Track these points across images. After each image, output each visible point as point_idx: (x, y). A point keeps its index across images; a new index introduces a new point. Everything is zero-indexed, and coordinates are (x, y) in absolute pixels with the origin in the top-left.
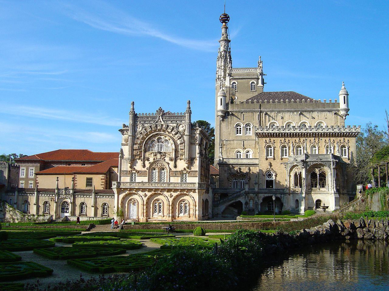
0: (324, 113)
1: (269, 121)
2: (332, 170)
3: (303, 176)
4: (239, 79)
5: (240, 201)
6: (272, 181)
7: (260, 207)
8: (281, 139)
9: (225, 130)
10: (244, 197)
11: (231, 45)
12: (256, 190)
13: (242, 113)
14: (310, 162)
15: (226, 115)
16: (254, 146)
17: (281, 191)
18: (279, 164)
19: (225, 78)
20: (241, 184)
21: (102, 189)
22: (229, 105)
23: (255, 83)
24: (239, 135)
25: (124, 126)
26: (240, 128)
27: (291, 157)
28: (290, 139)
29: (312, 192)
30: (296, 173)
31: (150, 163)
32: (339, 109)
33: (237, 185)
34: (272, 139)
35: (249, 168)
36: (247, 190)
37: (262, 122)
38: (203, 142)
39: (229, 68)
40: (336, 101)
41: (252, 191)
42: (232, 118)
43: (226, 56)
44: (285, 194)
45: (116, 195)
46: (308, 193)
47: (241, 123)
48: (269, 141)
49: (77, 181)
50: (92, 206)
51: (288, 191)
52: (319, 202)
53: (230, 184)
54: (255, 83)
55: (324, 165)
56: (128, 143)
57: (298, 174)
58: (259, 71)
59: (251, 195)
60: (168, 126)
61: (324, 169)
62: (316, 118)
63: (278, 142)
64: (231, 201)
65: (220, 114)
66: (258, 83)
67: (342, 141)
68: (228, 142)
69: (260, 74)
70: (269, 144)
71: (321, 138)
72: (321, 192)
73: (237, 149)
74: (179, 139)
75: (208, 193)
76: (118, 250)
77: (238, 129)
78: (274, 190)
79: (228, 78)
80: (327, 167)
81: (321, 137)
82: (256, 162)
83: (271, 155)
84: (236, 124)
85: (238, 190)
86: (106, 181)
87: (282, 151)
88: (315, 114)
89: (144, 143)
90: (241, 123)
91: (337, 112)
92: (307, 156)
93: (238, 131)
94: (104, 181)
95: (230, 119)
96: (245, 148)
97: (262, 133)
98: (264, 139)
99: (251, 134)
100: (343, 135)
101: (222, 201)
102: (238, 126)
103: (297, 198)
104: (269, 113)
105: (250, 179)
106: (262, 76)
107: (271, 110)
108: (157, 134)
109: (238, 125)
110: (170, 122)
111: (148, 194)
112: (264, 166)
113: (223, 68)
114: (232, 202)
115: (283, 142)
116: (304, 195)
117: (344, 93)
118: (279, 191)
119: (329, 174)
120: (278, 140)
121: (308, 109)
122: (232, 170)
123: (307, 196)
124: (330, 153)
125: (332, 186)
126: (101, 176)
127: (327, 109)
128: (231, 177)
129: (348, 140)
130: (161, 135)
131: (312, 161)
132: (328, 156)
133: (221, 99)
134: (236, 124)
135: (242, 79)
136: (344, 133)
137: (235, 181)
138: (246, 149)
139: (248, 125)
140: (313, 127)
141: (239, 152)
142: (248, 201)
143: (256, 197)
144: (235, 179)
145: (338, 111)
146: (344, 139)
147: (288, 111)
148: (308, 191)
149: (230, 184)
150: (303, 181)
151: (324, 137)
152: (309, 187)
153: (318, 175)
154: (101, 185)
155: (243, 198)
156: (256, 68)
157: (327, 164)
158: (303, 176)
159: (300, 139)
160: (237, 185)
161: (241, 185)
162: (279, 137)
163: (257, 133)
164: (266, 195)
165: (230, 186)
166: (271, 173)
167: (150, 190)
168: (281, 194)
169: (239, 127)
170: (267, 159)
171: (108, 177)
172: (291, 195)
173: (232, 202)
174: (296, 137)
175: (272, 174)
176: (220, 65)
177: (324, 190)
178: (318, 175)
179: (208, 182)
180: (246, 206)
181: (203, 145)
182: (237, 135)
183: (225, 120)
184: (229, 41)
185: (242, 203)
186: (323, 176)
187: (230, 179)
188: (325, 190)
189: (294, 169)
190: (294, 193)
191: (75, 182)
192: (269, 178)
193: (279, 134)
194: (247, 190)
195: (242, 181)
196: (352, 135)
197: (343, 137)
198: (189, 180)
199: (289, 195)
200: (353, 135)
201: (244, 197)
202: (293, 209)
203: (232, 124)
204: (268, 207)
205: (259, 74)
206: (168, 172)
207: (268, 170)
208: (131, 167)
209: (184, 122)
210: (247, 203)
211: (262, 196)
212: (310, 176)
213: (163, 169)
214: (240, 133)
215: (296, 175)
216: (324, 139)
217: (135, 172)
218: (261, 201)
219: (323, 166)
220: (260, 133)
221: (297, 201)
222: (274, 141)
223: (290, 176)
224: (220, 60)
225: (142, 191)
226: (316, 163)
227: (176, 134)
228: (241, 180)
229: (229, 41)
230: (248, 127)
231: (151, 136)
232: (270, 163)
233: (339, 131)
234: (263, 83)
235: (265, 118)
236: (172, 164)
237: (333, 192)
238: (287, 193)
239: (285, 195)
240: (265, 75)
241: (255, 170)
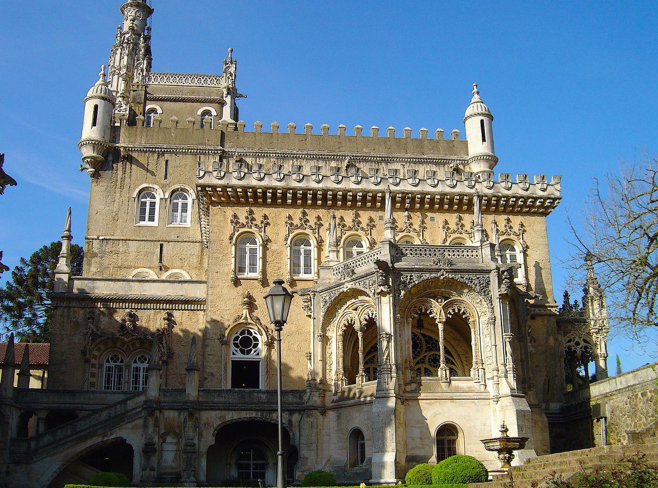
2: (497, 303)
3: (386, 322)
5: (122, 442)
6: (256, 364)
7: (204, 463)
8: (291, 211)
9: (101, 207)
10: (140, 422)
11: (152, 21)
14: (411, 270)
15: (108, 158)
16: (195, 260)
20: (136, 377)
22: (122, 130)
24: (146, 223)
26: (153, 205)
27: (327, 267)
28: (321, 212)
29: (423, 395)
32: (465, 158)
34: (259, 212)
35: (170, 315)
36: (153, 392)
39: (142, 71)
40: (457, 135)
41: (174, 397)
42: (128, 171)
43: (136, 44)
44: (305, 410)
46: (409, 395)
47: (156, 187)
48: (247, 218)
51: (316, 400)
52: (448, 432)
53: (93, 375)
54: (214, 113)
55: (464, 285)
57: (357, 326)
58: (224, 83)
59: (171, 414)
61: (461, 302)
63: (280, 219)
65: (88, 152)
66: (220, 115)
68: (109, 247)
69: (228, 89)
70: (246, 229)
71: (430, 215)
72: (455, 395)
78: (264, 396)
80: (473, 294)
81: (431, 209)
82: (197, 292)
83: (253, 270)
84: (138, 190)
87: (295, 254)
90: (156, 187)
91: (461, 167)
92: (396, 251)
93: (143, 211)
95: (120, 173)
97: (224, 188)
98: (230, 211)
99: (188, 224)
100: (506, 205)
101: (47, 438)
103: (358, 420)
104: (249, 160)
106: (233, 98)
107: (256, 150)
112: (226, 308)
113: (124, 71)
114: (90, 442)
115: (296, 222)
116: (392, 403)
117: (480, 111)
119: (484, 319)
120: (279, 216)
121: (372, 154)
122: (104, 320)
123: (401, 408)
124: (482, 241)
125: (502, 368)
128: (99, 350)
129: (522, 225)
131: (418, 270)
132: (474, 253)
133: (96, 107)
134: (141, 187)
136: (508, 198)
137: (112, 364)
138: (167, 269)
142: (156, 439)
143: (189, 423)
145: (466, 163)
146: (509, 220)
148: (405, 392)
149: (93, 375)
150: (385, 344)
151: (441, 210)
152: (409, 374)
153: (441, 327)
156: (218, 78)
157: (477, 282)
158: (386, 322)
159: (357, 215)
162: (284, 204)
163: (204, 187)
165: (92, 385)
166: (250, 333)
169: (148, 200)
170: (237, 282)
172: (331, 415)
173: (90, 442)
174: (344, 206)
175: (256, 339)
176: (117, 63)
178: (441, 327)
182: (142, 223)
183: (106, 174)
184: (149, 12)
185: (130, 447)
186: (459, 328)
187: (95, 357)
189: (341, 312)
190: (344, 403)
192: (243, 352)
193: (285, 191)
194: (153, 392)
196: (533, 206)
197: (504, 212)
199: (323, 413)
200: (539, 207)
201: (140, 422)
203: (126, 188)
204: (239, 467)
205: (225, 92)
207: (241, 321)
210: (149, 449)
214: (152, 219)
215: (349, 333)
216: (440, 218)
218: (209, 439)
219: (460, 287)
220: (214, 187)
221: (357, 434)
222: (265, 217)
223: (325, 340)
224: (119, 52)
226: (433, 275)
228: (135, 362)
230: (180, 202)
232: (250, 297)
233: (491, 191)
234: (235, 115)
237: (508, 392)
238: (315, 408)
239: (308, 416)
240: (241, 96)
241: (191, 323)
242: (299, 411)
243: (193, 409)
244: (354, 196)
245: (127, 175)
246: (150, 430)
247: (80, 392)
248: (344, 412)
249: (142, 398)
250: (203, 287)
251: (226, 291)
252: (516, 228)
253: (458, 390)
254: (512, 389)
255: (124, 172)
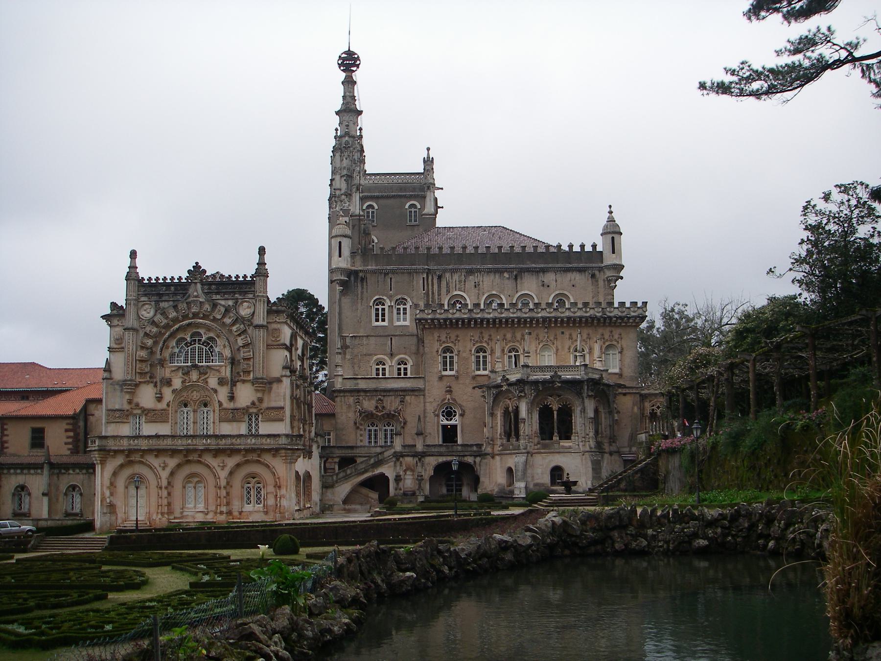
0: (569, 276)
1: (448, 292)
3: (523, 413)
4: (382, 197)
7: (428, 486)
10: (392, 464)
12: (420, 448)
13: (386, 274)
16: (414, 348)
17: (475, 448)
18: (470, 389)
19: (349, 195)
20: (386, 435)
21: (69, 452)
23: (419, 207)
24: (380, 323)
25: (114, 305)
26: (383, 310)
28: (492, 332)
30: (507, 408)
31: (174, 391)
33: (376, 438)
37: (433, 293)
38: (296, 340)
44: (483, 455)
45: (98, 469)
49: (7, 435)
50: (44, 494)
54: (419, 207)
56: (123, 345)
57: (510, 409)
59: (409, 460)
60: (215, 306)
62: (551, 286)
64: (363, 473)
66: (423, 207)
67: (607, 337)
68: (357, 341)
73: (375, 358)
74: (239, 335)
75: (310, 458)
76: (87, 594)
77: (377, 310)
78: (459, 448)
79: (356, 197)
85: (379, 450)
86: (77, 435)
88: (550, 278)
89: (161, 345)
93: (377, 315)
94: (71, 434)
95: (360, 288)
96: (392, 355)
97: (432, 320)
99: (407, 323)
102: (377, 305)
105: (405, 423)
107: (451, 267)
108: (189, 325)
109: (379, 302)
110: (218, 297)
111: (172, 463)
115: (477, 339)
118: (469, 449)
119: (579, 408)
126: (64, 425)
127: (575, 265)
130: (198, 325)
133: (340, 243)
135: (388, 197)
139: (403, 301)
140: (544, 306)
141: (381, 362)
142: (401, 473)
144: (373, 425)
147: (489, 271)
149: (361, 435)
153: (555, 413)
154: (66, 444)
155: (389, 467)
160: (376, 438)
161: (386, 438)
163: (420, 320)
164: (441, 459)
165: (361, 441)
167: (174, 452)
168: (475, 456)
169: (380, 307)
171: (81, 424)
172: (498, 458)
177: (571, 444)
178: (555, 413)
179: (310, 432)
180: (398, 484)
181: (297, 349)
182: (377, 324)
184: (360, 113)
186: (566, 414)
188: (571, 444)
191: (5, 438)
192: (447, 420)
195: (389, 428)
198: (265, 428)
199: (493, 457)
202: (502, 490)
203: (365, 299)
204: (447, 486)
206: (217, 411)
208: (130, 402)
209: (251, 296)
210: (398, 479)
211: (432, 462)
212: (536, 416)
213: (206, 405)
214: (383, 320)
215: (506, 412)
217: (139, 412)
220: (426, 320)
223: (492, 415)
225: (156, 456)
227: (233, 324)
229: (360, 113)
231: (178, 330)
235: (439, 287)
236: (223, 393)
242: (479, 456)
243: (421, 456)
244: (513, 321)
245: (365, 287)
246: (398, 468)
247: (357, 447)
248: (504, 457)
249: (393, 450)
250: (422, 381)
251: (436, 383)
252: (616, 337)
253: (563, 447)
254: (591, 448)
255: (363, 288)
